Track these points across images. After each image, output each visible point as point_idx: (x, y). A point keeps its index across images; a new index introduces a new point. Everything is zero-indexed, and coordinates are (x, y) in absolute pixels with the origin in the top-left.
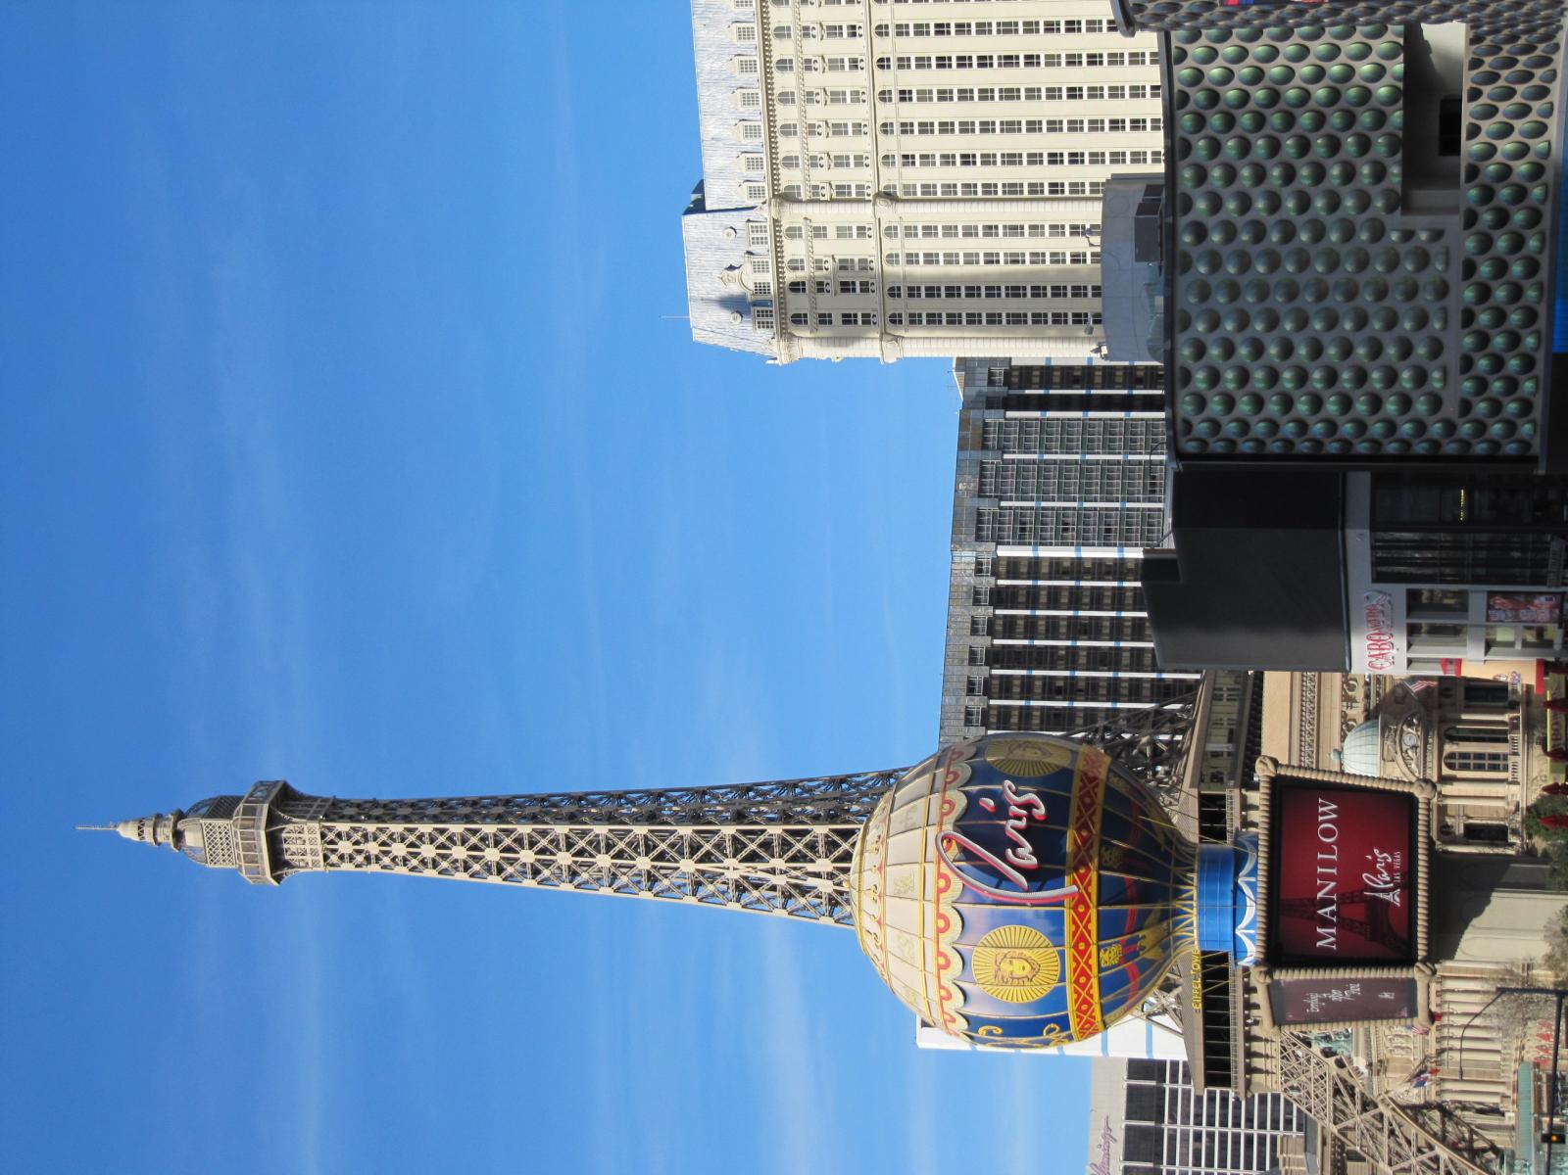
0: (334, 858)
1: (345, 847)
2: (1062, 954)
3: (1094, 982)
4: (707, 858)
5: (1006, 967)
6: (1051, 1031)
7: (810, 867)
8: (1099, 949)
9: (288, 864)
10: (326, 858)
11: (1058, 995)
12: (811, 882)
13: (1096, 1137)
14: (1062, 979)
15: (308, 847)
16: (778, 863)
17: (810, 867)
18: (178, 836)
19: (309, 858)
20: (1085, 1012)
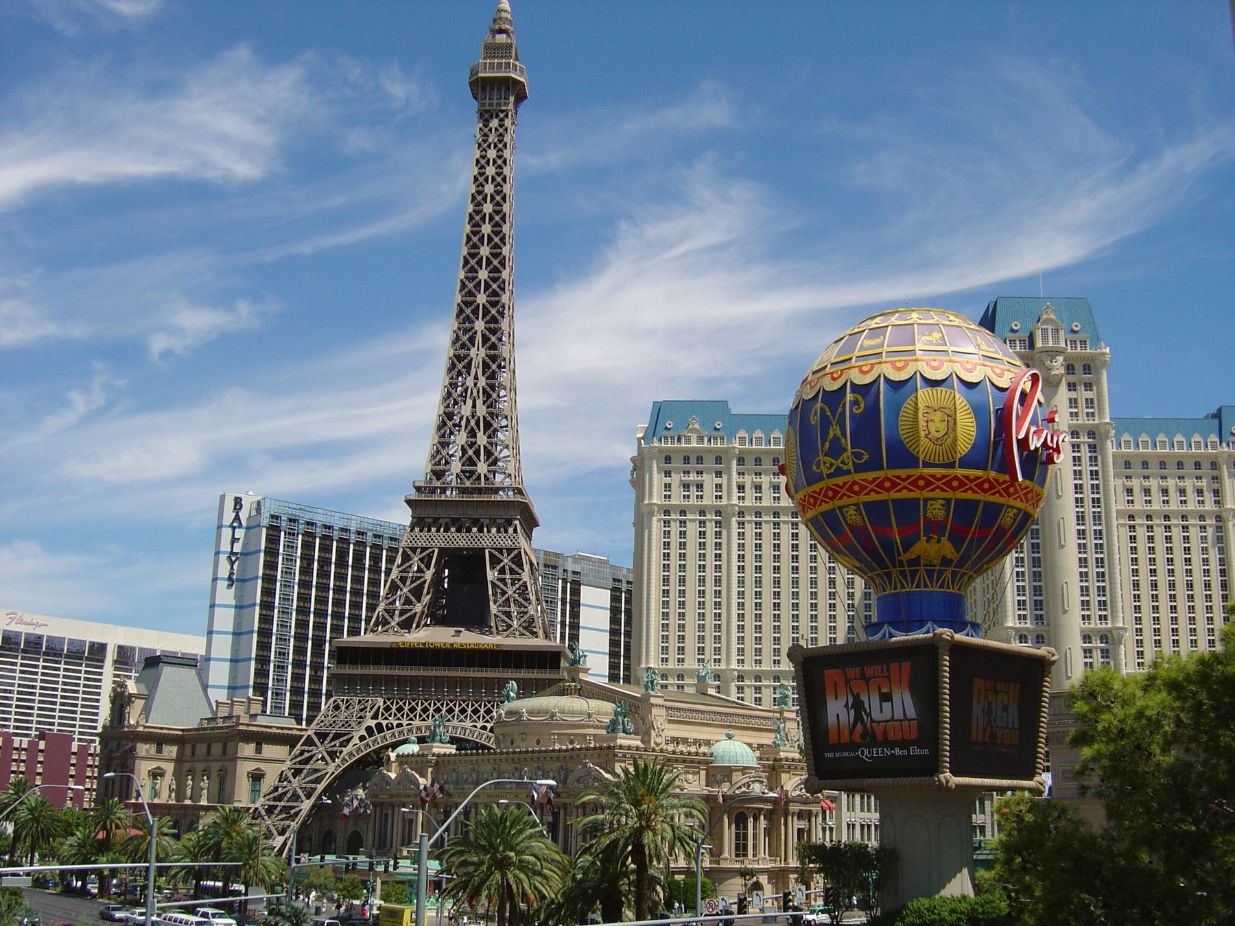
0: (487, 116)
2: (951, 465)
3: (915, 494)
4: (485, 339)
5: (938, 416)
6: (858, 456)
8: (948, 501)
9: (484, 89)
10: (487, 111)
11: (912, 461)
13: (38, 619)
14: (926, 465)
15: (495, 101)
16: (482, 382)
17: (479, 402)
19: (487, 101)
20: (825, 495)
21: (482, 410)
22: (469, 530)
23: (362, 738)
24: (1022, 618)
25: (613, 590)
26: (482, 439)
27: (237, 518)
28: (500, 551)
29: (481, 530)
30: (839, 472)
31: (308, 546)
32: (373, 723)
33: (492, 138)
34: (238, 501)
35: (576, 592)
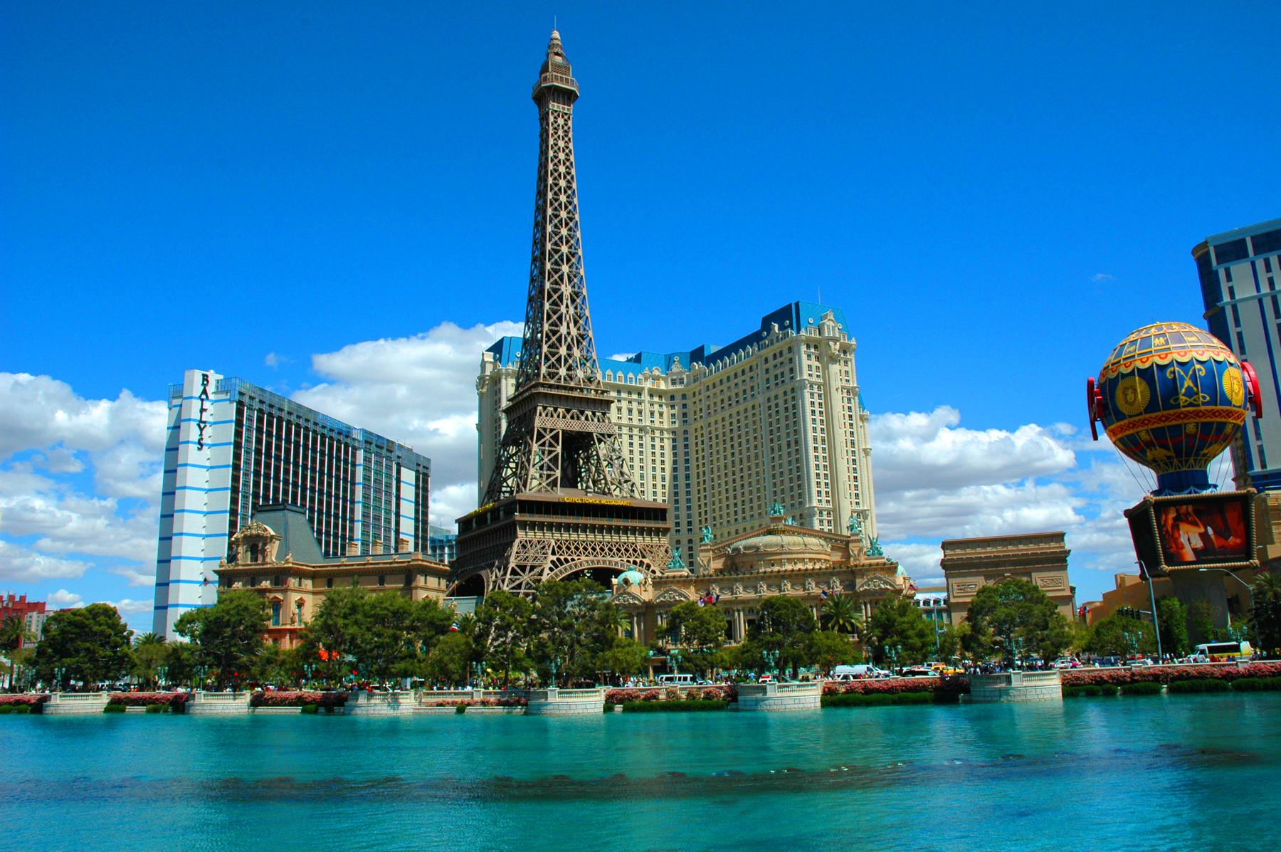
1: (561, 121)
7: (572, 325)
11: (1229, 403)
12: (565, 324)
16: (572, 310)
17: (572, 325)
18: (557, 54)
21: (574, 332)
22: (578, 418)
23: (551, 569)
24: (820, 501)
25: (417, 472)
26: (576, 352)
27: (205, 392)
28: (603, 435)
29: (587, 419)
30: (1190, 405)
31: (260, 420)
32: (554, 558)
33: (561, 133)
34: (205, 378)
35: (399, 472)
